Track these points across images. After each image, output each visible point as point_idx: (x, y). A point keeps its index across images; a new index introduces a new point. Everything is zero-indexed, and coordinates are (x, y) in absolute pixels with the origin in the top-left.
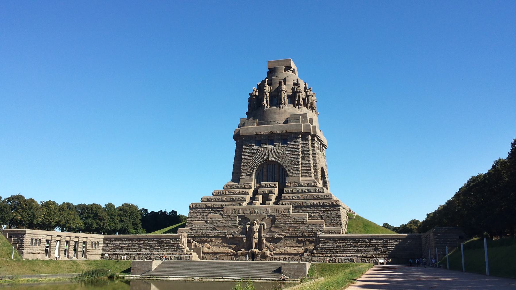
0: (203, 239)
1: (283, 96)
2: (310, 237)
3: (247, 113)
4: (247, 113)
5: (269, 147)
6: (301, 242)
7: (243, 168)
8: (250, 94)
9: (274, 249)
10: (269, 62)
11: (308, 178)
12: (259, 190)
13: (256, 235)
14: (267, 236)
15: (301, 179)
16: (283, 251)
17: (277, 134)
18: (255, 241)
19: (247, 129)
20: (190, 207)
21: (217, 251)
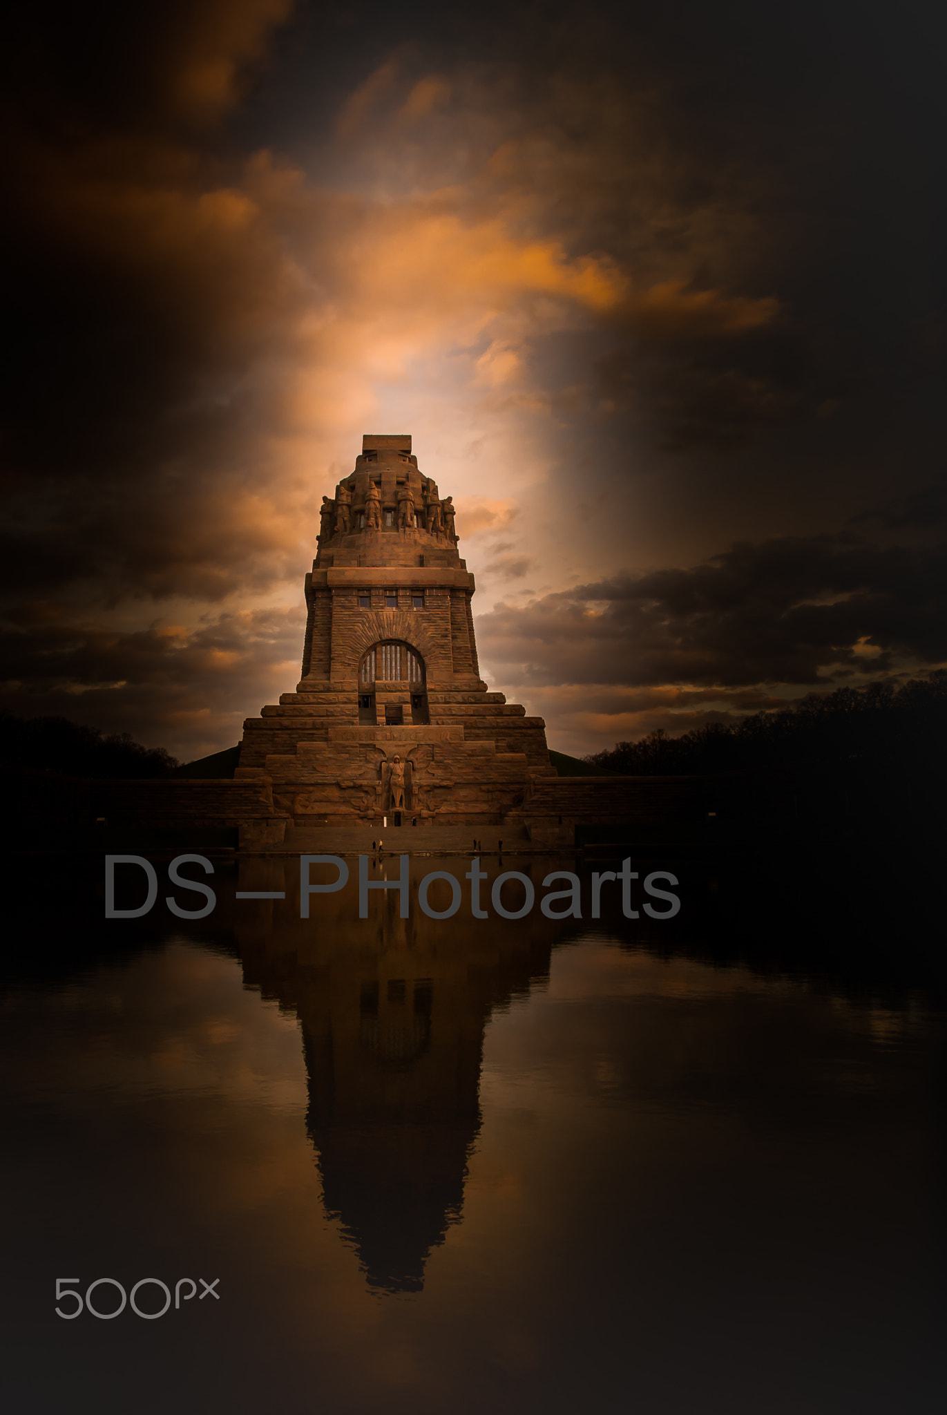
0: (292, 789)
1: (409, 512)
2: (502, 784)
3: (318, 538)
4: (318, 538)
5: (389, 612)
6: (489, 791)
7: (337, 650)
8: (325, 499)
9: (437, 807)
10: (366, 438)
11: (467, 676)
12: (380, 697)
13: (401, 780)
14: (423, 782)
15: (458, 676)
16: (454, 809)
17: (404, 588)
18: (398, 794)
19: (343, 572)
20: (245, 727)
21: (323, 811)
